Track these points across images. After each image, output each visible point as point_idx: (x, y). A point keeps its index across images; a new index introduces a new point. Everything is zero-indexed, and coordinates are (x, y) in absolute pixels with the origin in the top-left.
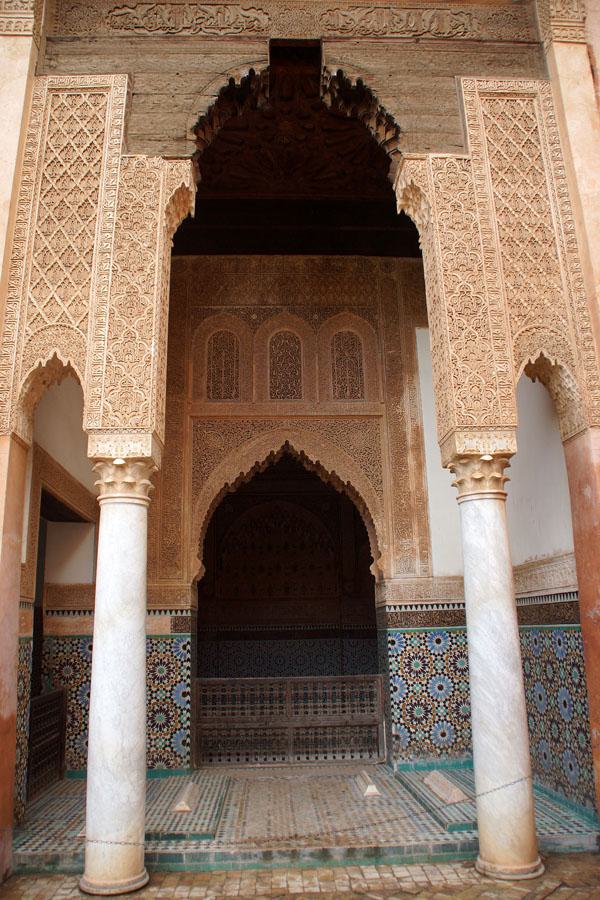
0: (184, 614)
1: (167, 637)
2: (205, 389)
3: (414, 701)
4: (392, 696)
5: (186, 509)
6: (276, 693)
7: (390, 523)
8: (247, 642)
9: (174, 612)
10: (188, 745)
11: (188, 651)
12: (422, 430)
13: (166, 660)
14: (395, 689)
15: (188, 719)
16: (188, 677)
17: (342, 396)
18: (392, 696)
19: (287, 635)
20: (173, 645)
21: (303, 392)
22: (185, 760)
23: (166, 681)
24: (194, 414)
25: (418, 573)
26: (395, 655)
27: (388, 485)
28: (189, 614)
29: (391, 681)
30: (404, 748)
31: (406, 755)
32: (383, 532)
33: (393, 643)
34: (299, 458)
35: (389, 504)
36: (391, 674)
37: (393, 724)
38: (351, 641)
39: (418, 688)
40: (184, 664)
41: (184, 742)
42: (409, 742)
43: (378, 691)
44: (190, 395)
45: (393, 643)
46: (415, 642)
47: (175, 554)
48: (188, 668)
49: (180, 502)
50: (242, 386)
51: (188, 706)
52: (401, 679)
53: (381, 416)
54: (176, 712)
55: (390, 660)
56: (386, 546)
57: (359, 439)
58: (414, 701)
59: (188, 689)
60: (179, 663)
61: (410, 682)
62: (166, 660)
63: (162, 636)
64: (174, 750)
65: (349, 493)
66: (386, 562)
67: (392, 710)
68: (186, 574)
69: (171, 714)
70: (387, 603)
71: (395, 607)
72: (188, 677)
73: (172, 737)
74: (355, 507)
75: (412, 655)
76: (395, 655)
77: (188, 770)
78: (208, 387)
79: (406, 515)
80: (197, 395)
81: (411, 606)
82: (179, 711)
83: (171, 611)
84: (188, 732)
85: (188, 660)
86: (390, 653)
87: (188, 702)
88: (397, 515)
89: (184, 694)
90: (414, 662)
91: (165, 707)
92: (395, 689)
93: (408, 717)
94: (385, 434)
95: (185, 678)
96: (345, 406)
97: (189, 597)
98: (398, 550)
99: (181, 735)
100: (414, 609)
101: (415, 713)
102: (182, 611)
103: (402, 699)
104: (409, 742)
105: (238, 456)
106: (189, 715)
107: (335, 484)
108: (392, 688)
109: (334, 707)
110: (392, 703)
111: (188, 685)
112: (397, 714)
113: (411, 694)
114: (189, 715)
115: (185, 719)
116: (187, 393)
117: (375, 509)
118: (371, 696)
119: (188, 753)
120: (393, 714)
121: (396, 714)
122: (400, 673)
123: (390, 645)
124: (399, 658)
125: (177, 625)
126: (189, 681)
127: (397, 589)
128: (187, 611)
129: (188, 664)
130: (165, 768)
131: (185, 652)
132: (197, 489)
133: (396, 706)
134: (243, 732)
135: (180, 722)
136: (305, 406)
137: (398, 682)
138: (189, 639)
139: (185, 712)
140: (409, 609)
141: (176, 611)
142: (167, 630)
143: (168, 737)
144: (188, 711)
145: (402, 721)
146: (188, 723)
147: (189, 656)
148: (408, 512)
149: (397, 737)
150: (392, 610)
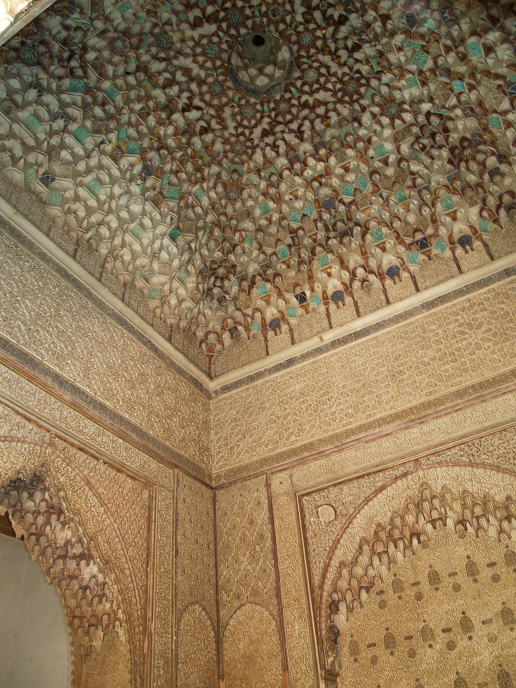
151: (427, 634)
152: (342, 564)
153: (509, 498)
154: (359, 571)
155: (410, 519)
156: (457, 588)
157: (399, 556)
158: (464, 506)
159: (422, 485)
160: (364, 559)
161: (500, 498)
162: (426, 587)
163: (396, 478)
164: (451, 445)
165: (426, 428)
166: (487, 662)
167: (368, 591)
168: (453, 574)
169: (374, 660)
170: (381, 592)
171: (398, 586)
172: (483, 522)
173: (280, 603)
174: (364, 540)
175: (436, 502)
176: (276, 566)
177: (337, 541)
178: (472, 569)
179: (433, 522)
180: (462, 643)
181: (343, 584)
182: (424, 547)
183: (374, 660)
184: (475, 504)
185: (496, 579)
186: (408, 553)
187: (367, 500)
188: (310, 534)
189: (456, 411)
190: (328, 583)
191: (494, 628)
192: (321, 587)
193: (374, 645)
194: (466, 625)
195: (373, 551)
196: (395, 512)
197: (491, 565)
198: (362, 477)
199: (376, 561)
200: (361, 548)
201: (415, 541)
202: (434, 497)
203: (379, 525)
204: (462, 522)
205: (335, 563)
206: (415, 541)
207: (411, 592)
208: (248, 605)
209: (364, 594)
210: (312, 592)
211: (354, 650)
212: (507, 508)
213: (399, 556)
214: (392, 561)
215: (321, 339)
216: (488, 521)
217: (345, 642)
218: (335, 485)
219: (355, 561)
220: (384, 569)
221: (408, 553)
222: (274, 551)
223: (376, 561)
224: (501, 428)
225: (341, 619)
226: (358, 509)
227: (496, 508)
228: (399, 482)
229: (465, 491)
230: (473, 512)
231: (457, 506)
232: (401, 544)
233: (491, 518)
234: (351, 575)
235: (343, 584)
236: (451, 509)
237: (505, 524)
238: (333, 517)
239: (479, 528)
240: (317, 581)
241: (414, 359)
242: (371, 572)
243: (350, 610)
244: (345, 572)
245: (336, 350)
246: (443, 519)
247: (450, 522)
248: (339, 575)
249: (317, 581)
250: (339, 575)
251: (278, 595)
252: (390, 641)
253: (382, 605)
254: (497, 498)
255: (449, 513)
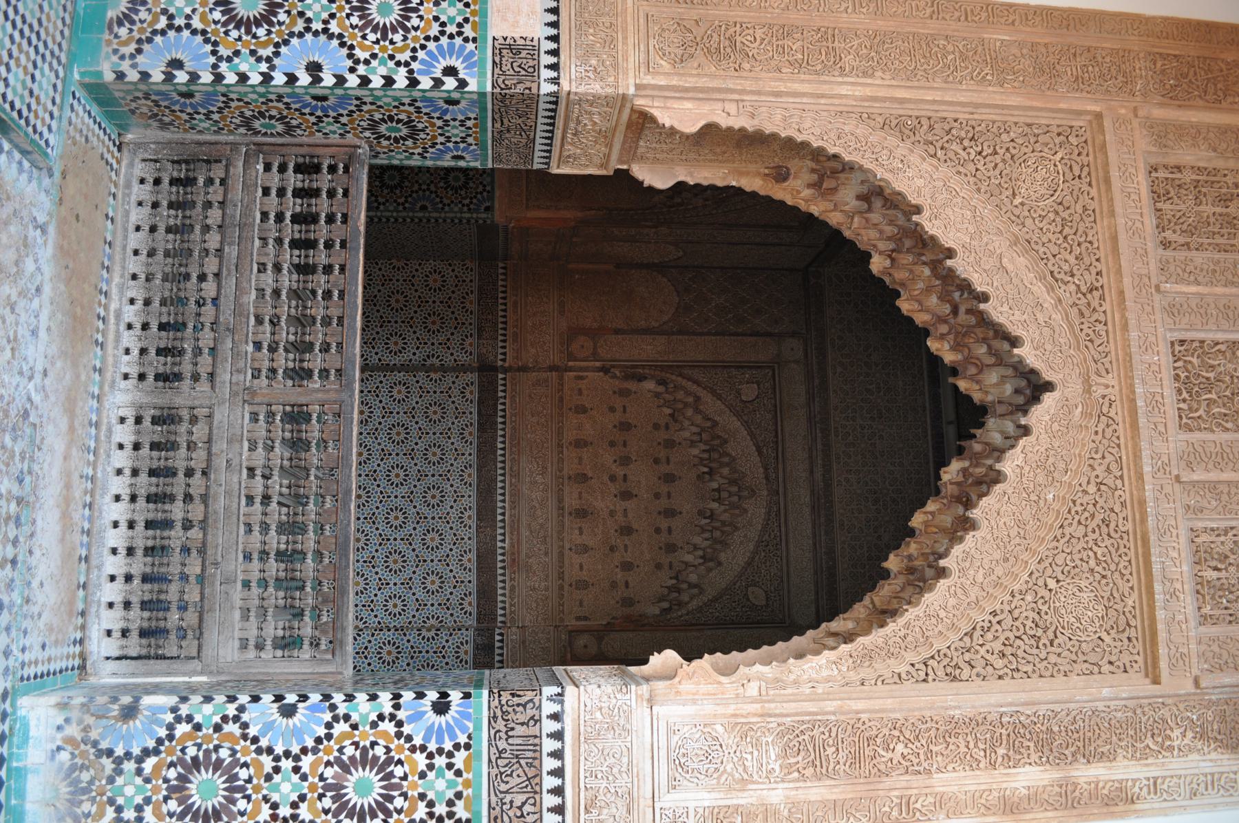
0: (546, 74)
1: (481, 26)
2: (1172, 160)
3: (243, 774)
4: (267, 698)
5: (849, 89)
6: (316, 361)
7: (830, 706)
8: (474, 429)
9: (552, 46)
10: (169, 77)
11: (438, 83)
12: (1124, 815)
13: (415, 21)
14: (288, 711)
15: (243, 78)
16: (365, 81)
17: (1200, 557)
18: (267, 698)
19: (486, 512)
20: (458, 41)
21: (1197, 436)
22: (125, 66)
23: (355, 20)
24: (1107, 123)
25: (668, 800)
26: (401, 715)
27: (951, 701)
28: (546, 88)
29: (315, 698)
30: (94, 735)
31: (70, 740)
32: (796, 683)
33: (441, 707)
34: (977, 447)
35: (889, 703)
36: (338, 698)
37: (173, 700)
38: (469, 648)
39: (286, 788)
40: (403, 71)
41: (177, 64)
42: (110, 753)
43: (302, 664)
44: (1158, 113)
45: (441, 707)
46: (440, 785)
47: (715, 54)
48: (389, 81)
49: (865, 74)
50: (1199, 258)
51: (279, 79)
52: (322, 732)
53: (1156, 681)
54: (264, 45)
55: (385, 698)
56: (753, 689)
57: (1078, 605)
58: (243, 774)
59: (328, 80)
60: (404, 56)
61: (306, 763)
62: (415, 21)
63: (484, 14)
64: (158, 39)
65: (885, 590)
66: (704, 688)
67: (220, 699)
68: (662, 81)
69: (261, 32)
70: (570, 690)
71: (556, 717)
72: (365, 81)
73: (194, 32)
74: (847, 608)
75: (399, 771)
76: (401, 715)
77: (99, 74)
78: (1179, 168)
79: (856, 760)
80: (1162, 134)
81: (558, 773)
82: (267, 52)
83: (555, 39)
84: (207, 78)
85: (413, 83)
86: (408, 696)
87: (292, 79)
88: (856, 725)
89: (314, 69)
90: (373, 777)
91: (282, 17)
92: (288, 711)
93: (192, 751)
94: (1106, 692)
95: (361, 69)
96: (1174, 563)
97: (596, 88)
98: (744, 730)
99: (198, 58)
100: (550, 782)
101: (205, 775)
102: (554, 67)
103: (252, 731)
104: (110, 753)
105: (1000, 244)
106: (255, 79)
107: (913, 547)
108: (291, 698)
109: (265, 528)
110: (244, 699)
111: (341, 80)
112: (207, 713)
113: (267, 762)
114: (255, 79)
115: (244, 67)
116: (1162, 105)
117: (869, 656)
118: (288, 644)
119: (145, 75)
120: (208, 699)
121: (208, 709)
122: (341, 728)
123: (432, 695)
124: (388, 727)
125: (510, 49)
126: (353, 81)
127: (618, 725)
128: (555, 81)
129: (401, 81)
130: (111, 14)
131: (438, 74)
132: (905, 127)
133: (231, 710)
134: (211, 265)
135: (237, 53)
136: (1163, 442)
137: (310, 721)
138: (473, 86)
139: (264, 67)
140: (550, 764)
141: (555, 53)
142: (498, 28)
143: (196, 23)
144: (267, 78)
145: (182, 729)
146: (231, 78)
147: (426, 83)
148: (867, 767)
149: (129, 712)
150: (549, 708)
151: (625, 461)
152: (698, 399)
153: (720, 564)
154: (689, 412)
155: (726, 471)
156: (657, 496)
157: (695, 452)
158: (724, 523)
159: (753, 491)
160: (698, 419)
161: (723, 557)
162: (664, 469)
163: (766, 469)
164: (783, 529)
165: (807, 511)
166: (595, 503)
167: (672, 415)
168: (669, 495)
169: (612, 409)
170: (667, 427)
171: (670, 444)
172: (707, 535)
173: (673, 333)
174: (715, 424)
175: (735, 499)
176: (709, 334)
177: (719, 398)
178: (670, 513)
179: (718, 490)
180: (613, 488)
181: (680, 395)
182: (698, 476)
183: (612, 409)
184: (723, 532)
185: (658, 531)
186: (696, 461)
187: (752, 435)
188: (734, 372)
189: (815, 544)
190: (684, 382)
191: (619, 517)
192: (680, 375)
193: (625, 411)
194: (626, 495)
195: (703, 430)
196: (734, 459)
197: (670, 530)
198: (776, 436)
199: (695, 429)
200: (709, 419)
201: (706, 470)
202: (740, 498)
203: (726, 442)
204: (712, 516)
205: (701, 392)
206: (706, 470)
207: (662, 455)
208: (677, 299)
209: (668, 411)
210: (678, 366)
211: (624, 393)
212: (711, 560)
213: (695, 452)
214: (693, 444)
215: (950, 423)
216: (707, 539)
217: (631, 385)
218: (775, 406)
219: (697, 411)
220: (687, 434)
221: (696, 461)
222: (723, 334)
223: (695, 429)
224: (785, 579)
225: (650, 385)
226: (746, 424)
227: (715, 550)
228: (761, 470)
229: (737, 529)
230: (717, 529)
231: (726, 517)
232: (706, 456)
233: (709, 542)
234: (686, 405)
235: (680, 395)
236: (725, 511)
237: (700, 553)
238: (744, 398)
239: (703, 530)
240: (686, 372)
241: (887, 519)
242: (686, 423)
243: (657, 395)
244: (691, 399)
245: (929, 438)
246: (718, 500)
247: (715, 505)
248: (688, 393)
249: (686, 372)
250: (688, 393)
251: (680, 332)
252: (625, 427)
253: (656, 426)
254: (723, 554)
255: (723, 508)
